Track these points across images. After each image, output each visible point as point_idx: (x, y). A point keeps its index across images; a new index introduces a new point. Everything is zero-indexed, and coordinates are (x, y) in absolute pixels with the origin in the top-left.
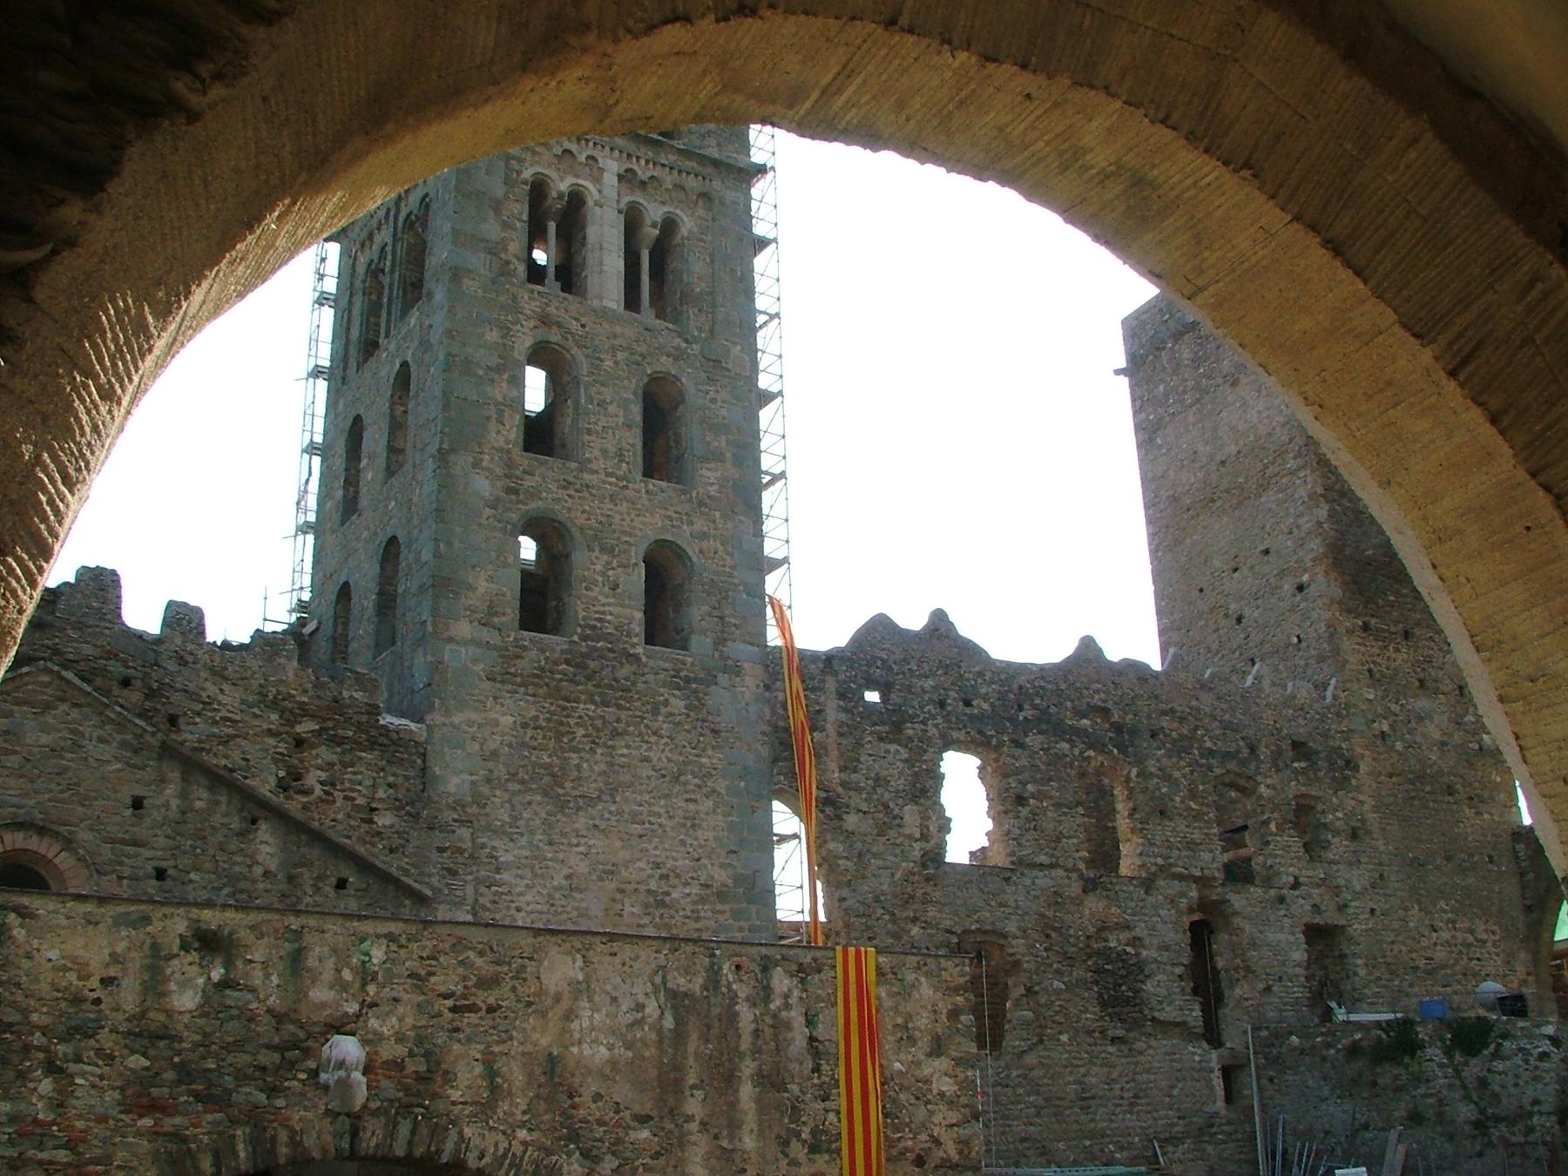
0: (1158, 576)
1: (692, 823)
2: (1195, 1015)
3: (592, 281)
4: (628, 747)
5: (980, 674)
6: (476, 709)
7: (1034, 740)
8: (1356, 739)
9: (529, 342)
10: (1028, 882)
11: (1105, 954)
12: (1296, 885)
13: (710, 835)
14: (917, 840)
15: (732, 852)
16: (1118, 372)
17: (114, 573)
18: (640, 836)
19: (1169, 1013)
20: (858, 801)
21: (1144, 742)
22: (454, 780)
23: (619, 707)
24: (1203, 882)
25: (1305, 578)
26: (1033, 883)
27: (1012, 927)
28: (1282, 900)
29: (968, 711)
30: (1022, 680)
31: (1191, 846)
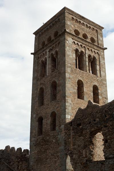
1: (56, 162)
4: (48, 151)
5: (97, 112)
6: (33, 151)
9: (39, 89)
10: (107, 163)
13: (57, 164)
14: (85, 158)
15: (60, 167)
17: (9, 146)
18: (49, 167)
20: (75, 152)
23: (48, 145)
26: (109, 163)
29: (95, 122)
30: (106, 109)
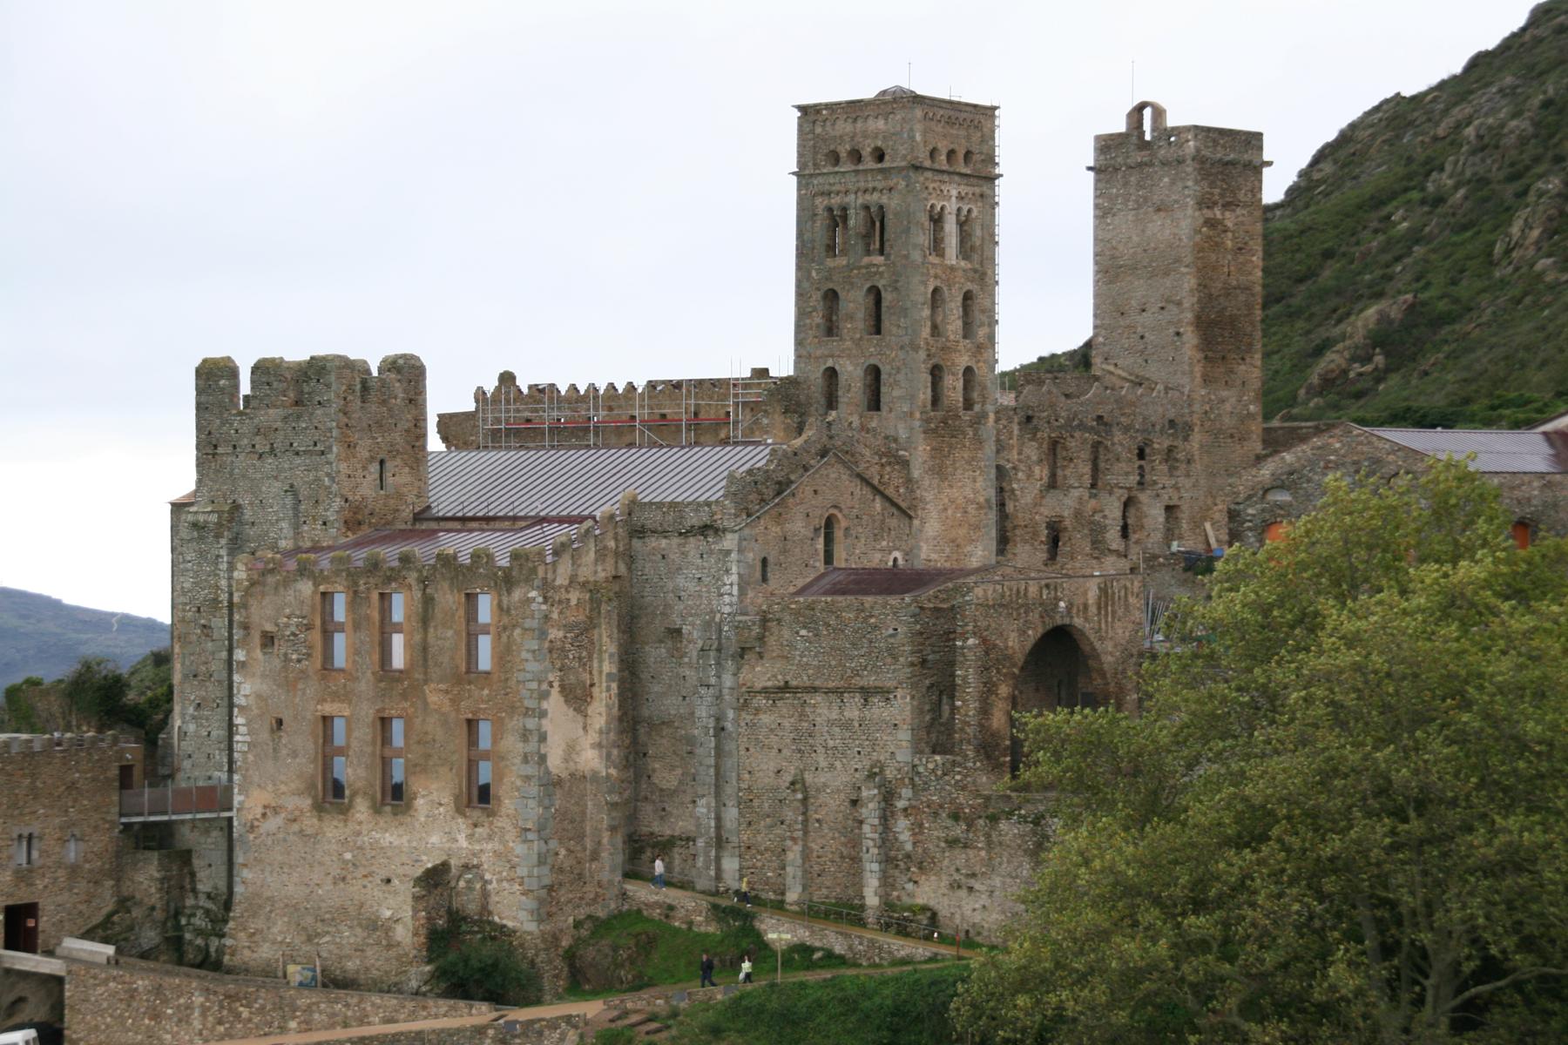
0: (1097, 295)
2: (1122, 548)
3: (948, 251)
7: (1077, 434)
8: (1195, 416)
11: (1092, 523)
12: (1164, 488)
16: (1089, 169)
19: (1114, 546)
21: (1115, 430)
22: (916, 474)
24: (1129, 489)
25: (1182, 330)
27: (1066, 514)
28: (1158, 495)
31: (1127, 474)
